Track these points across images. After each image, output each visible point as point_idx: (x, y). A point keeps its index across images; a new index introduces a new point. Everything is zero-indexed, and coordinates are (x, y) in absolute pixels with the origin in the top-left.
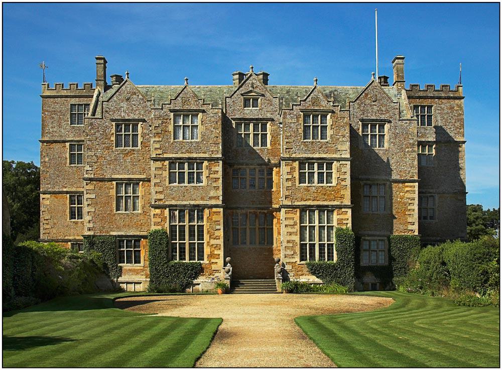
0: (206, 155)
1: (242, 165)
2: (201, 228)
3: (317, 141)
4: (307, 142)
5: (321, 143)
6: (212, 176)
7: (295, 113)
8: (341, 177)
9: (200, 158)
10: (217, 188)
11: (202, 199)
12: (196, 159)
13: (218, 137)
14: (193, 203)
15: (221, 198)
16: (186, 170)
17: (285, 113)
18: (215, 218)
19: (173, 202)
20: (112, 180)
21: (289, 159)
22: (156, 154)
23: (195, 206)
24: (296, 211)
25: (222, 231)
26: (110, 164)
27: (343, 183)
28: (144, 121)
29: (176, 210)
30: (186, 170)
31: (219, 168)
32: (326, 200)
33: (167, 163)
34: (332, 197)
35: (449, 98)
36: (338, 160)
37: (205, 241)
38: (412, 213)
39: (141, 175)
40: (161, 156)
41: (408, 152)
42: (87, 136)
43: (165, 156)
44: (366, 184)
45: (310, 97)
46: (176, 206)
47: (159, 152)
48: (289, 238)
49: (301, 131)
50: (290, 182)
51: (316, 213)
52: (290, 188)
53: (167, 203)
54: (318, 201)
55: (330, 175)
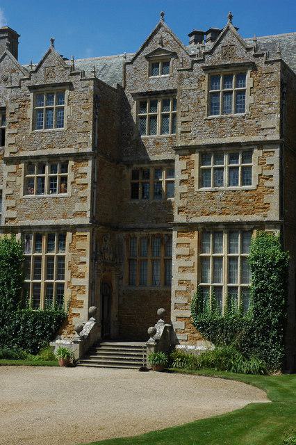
0: (72, 151)
1: (144, 163)
3: (229, 115)
4: (213, 119)
6: (79, 181)
7: (196, 74)
8: (266, 173)
10: (83, 199)
11: (64, 216)
12: (58, 156)
13: (87, 122)
15: (88, 214)
17: (181, 76)
19: (27, 223)
22: (11, 153)
23: (53, 227)
27: (268, 184)
29: (31, 232)
32: (240, 213)
34: (250, 208)
36: (260, 145)
40: (16, 155)
43: (22, 154)
45: (220, 46)
46: (29, 227)
47: (14, 149)
49: (204, 102)
51: (225, 236)
52: (185, 195)
53: (20, 224)
54: (227, 214)
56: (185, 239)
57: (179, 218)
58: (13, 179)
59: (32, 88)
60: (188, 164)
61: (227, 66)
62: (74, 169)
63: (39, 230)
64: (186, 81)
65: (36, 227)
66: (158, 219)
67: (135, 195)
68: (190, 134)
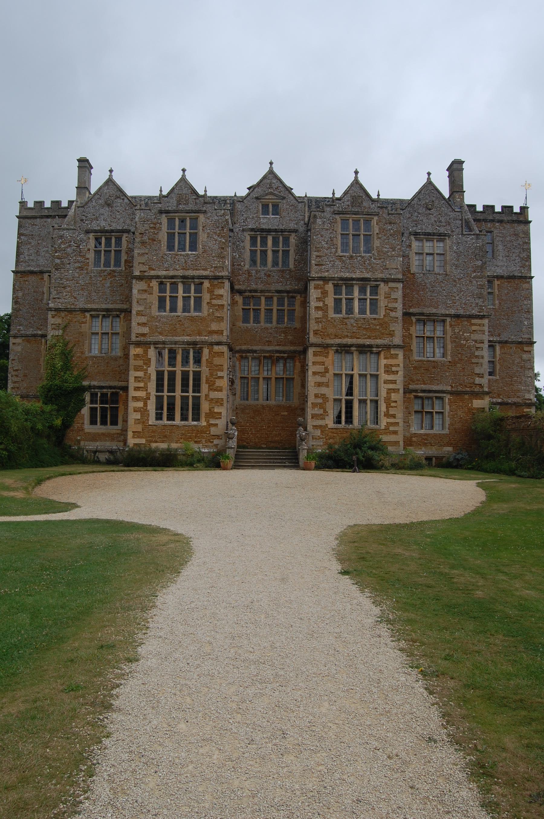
2: (197, 376)
5: (363, 257)
6: (215, 302)
9: (199, 277)
11: (200, 334)
12: (193, 278)
14: (186, 338)
16: (181, 293)
18: (217, 361)
19: (162, 338)
20: (84, 311)
23: (188, 343)
24: (328, 353)
25: (226, 379)
26: (82, 289)
27: (393, 314)
29: (164, 348)
30: (181, 293)
31: (225, 291)
32: (369, 337)
33: (154, 284)
35: (513, 222)
36: (386, 281)
37: (203, 394)
39: (122, 305)
40: (146, 274)
41: (474, 277)
42: (56, 252)
43: (152, 273)
46: (164, 343)
50: (320, 312)
54: (359, 338)
55: (374, 303)
56: (319, 359)
57: (313, 339)
58: (144, 296)
59: (161, 212)
60: (322, 293)
62: (210, 291)
63: (173, 346)
64: (319, 221)
65: (171, 343)
66: (269, 343)
67: (246, 320)
68: (323, 267)
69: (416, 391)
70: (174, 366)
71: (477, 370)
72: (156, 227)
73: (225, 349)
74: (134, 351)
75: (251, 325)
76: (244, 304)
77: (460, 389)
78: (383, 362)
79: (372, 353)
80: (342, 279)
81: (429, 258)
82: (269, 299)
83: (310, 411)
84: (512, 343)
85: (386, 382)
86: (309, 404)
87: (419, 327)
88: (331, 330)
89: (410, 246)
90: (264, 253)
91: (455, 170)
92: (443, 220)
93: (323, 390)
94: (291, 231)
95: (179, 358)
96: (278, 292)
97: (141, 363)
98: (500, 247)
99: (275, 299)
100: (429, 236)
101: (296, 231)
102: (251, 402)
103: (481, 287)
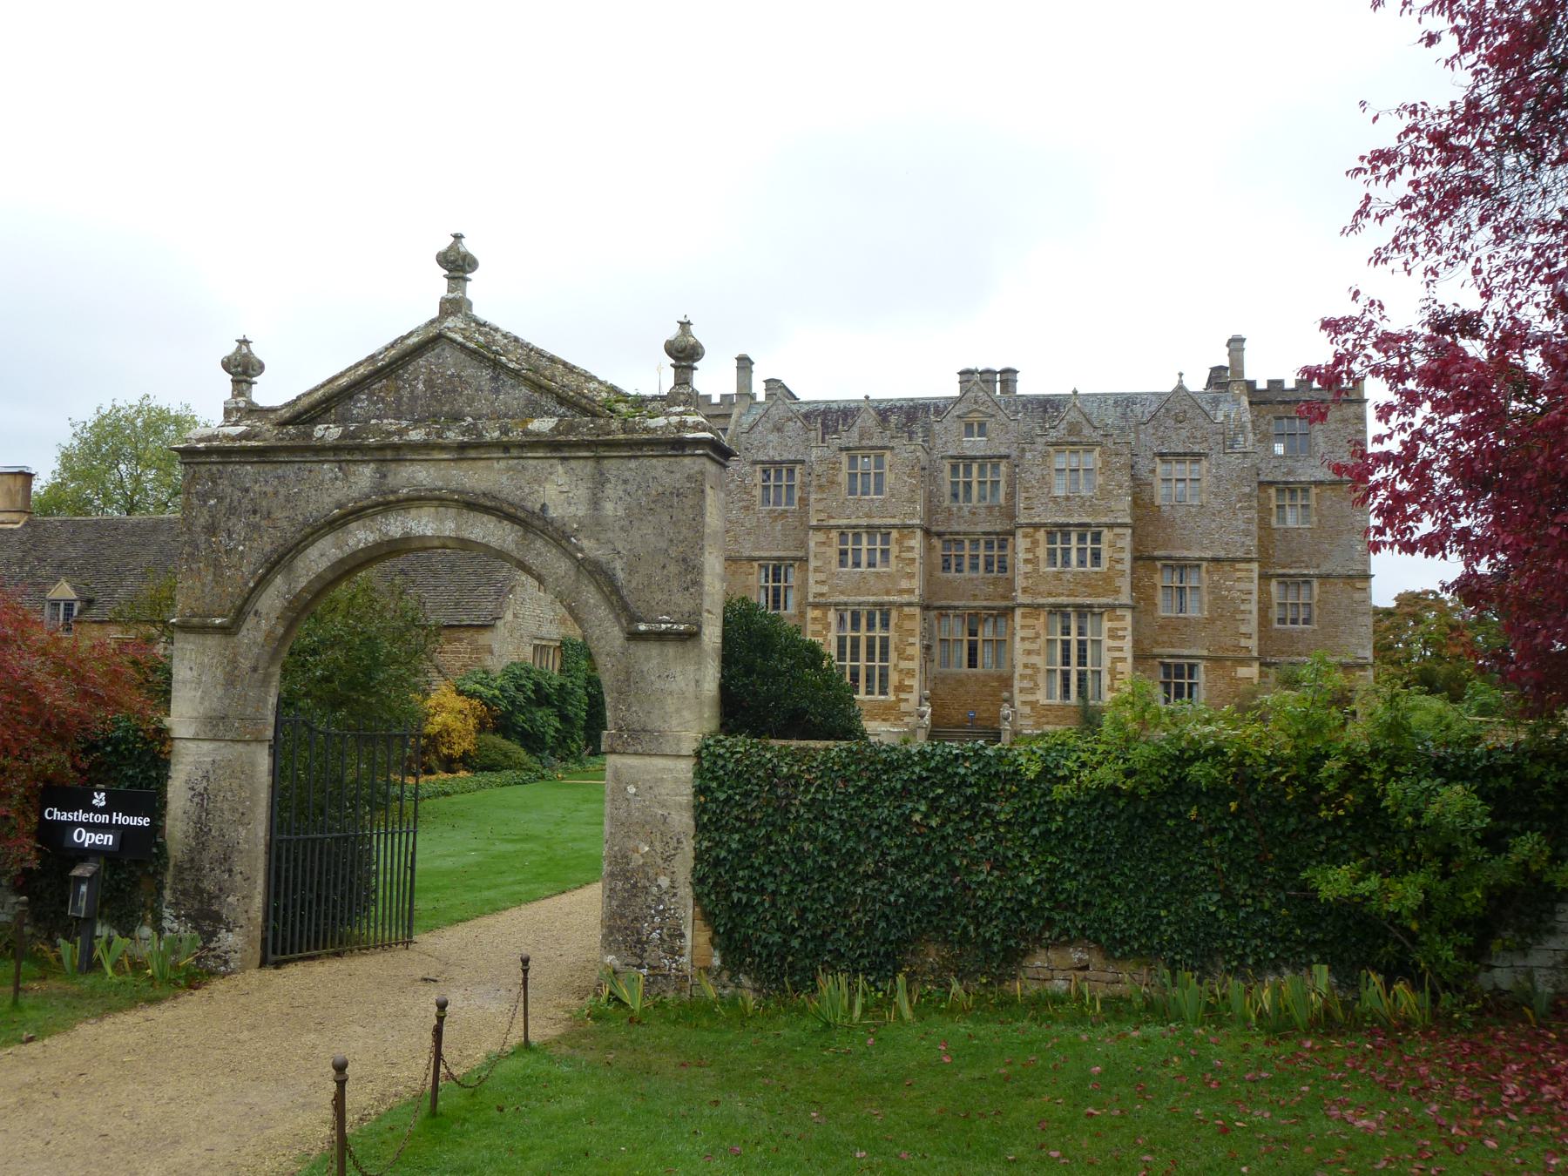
2: (885, 641)
8: (1116, 556)
9: (886, 527)
11: (888, 593)
12: (879, 527)
14: (872, 599)
19: (843, 598)
20: (751, 559)
21: (1029, 525)
23: (875, 604)
27: (1119, 567)
28: (802, 462)
30: (865, 545)
31: (916, 541)
32: (1090, 595)
33: (834, 534)
36: (1111, 526)
37: (890, 664)
38: (1247, 616)
41: (1241, 508)
43: (832, 522)
44: (1165, 566)
46: (846, 604)
47: (823, 516)
48: (1026, 659)
55: (1096, 556)
56: (1030, 622)
58: (823, 549)
59: (841, 449)
61: (1073, 444)
62: (899, 542)
64: (1028, 455)
65: (854, 604)
69: (1161, 656)
70: (858, 630)
71: (1243, 629)
72: (835, 465)
73: (917, 611)
74: (812, 614)
75: (952, 574)
76: (944, 549)
77: (1220, 654)
78: (1106, 625)
79: (1093, 614)
80: (1056, 525)
81: (1180, 485)
82: (975, 543)
83: (1017, 684)
84: (1339, 576)
85: (1110, 649)
86: (1017, 675)
87: (1167, 573)
88: (1043, 588)
89: (1153, 471)
90: (968, 485)
91: (1236, 345)
92: (1198, 434)
93: (1034, 659)
94: (1001, 457)
95: (863, 622)
96: (984, 533)
97: (819, 627)
98: (1321, 440)
99: (982, 543)
100: (1180, 457)
101: (1007, 457)
102: (954, 670)
103: (1249, 521)
